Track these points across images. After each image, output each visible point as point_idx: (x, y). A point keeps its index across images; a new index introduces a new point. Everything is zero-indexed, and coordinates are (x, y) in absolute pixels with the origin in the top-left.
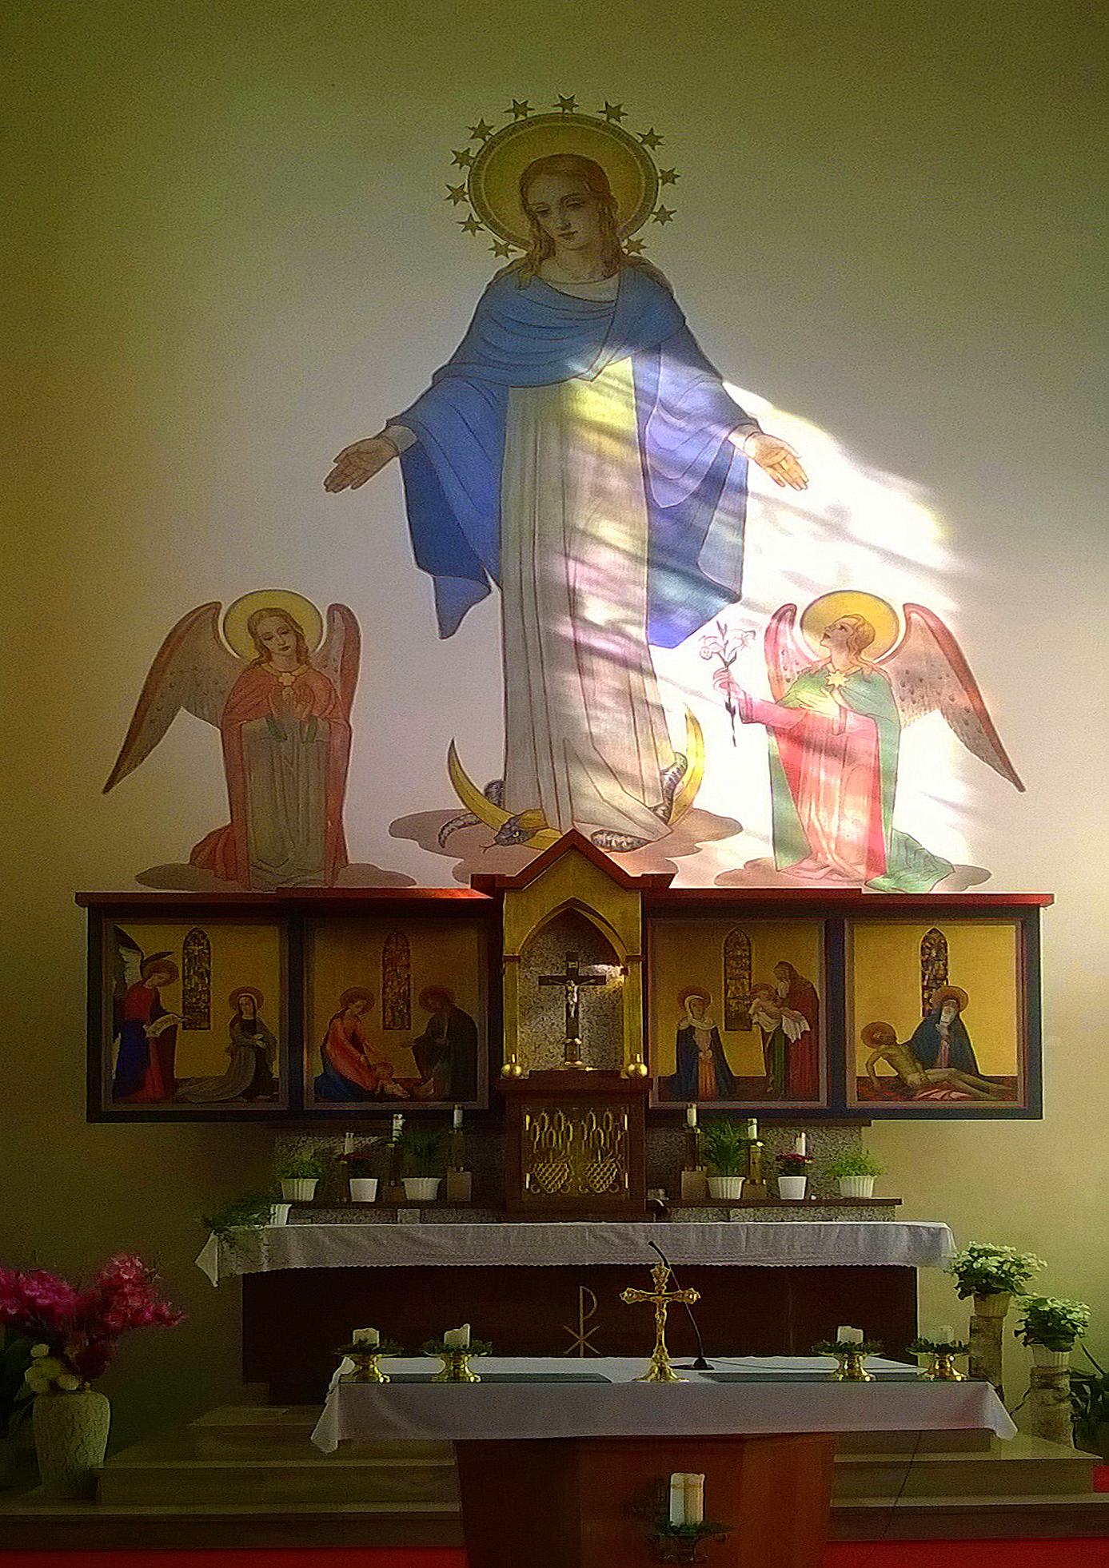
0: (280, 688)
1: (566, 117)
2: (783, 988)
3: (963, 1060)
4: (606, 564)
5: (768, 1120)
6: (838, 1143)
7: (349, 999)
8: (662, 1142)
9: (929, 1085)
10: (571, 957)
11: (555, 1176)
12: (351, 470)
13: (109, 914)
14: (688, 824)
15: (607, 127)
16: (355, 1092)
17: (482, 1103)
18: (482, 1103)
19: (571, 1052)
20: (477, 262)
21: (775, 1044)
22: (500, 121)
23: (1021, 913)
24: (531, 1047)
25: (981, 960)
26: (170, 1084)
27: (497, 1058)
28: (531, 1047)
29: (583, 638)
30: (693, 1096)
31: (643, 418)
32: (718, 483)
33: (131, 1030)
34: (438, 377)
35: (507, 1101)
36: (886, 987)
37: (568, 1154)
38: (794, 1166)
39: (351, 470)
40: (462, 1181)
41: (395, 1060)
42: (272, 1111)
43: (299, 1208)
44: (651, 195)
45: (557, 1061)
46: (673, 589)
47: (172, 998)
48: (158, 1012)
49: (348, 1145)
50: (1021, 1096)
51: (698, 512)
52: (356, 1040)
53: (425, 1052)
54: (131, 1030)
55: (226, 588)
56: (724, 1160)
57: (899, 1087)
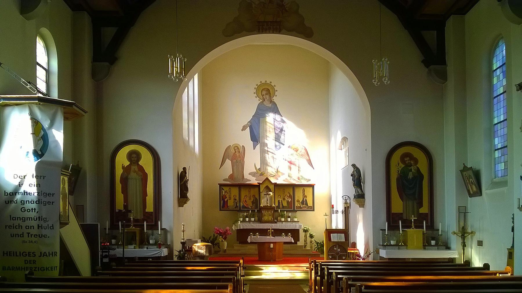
0: (236, 156)
3: (307, 204)
4: (270, 141)
5: (287, 211)
6: (294, 214)
8: (276, 213)
11: (266, 218)
12: (244, 129)
13: (221, 185)
14: (280, 174)
15: (270, 85)
16: (246, 208)
19: (267, 203)
20: (257, 102)
21: (288, 202)
22: (259, 84)
23: (312, 186)
24: (264, 203)
25: (309, 190)
26: (228, 206)
27: (260, 204)
28: (264, 203)
29: (269, 150)
31: (274, 122)
32: (282, 130)
33: (223, 200)
35: (260, 210)
36: (299, 195)
37: (267, 216)
38: (289, 217)
39: (244, 129)
40: (257, 218)
41: (250, 204)
42: (238, 209)
45: (266, 205)
46: (277, 144)
47: (227, 196)
50: (312, 209)
51: (280, 134)
53: (253, 203)
54: (223, 200)
55: (232, 143)
56: (282, 216)
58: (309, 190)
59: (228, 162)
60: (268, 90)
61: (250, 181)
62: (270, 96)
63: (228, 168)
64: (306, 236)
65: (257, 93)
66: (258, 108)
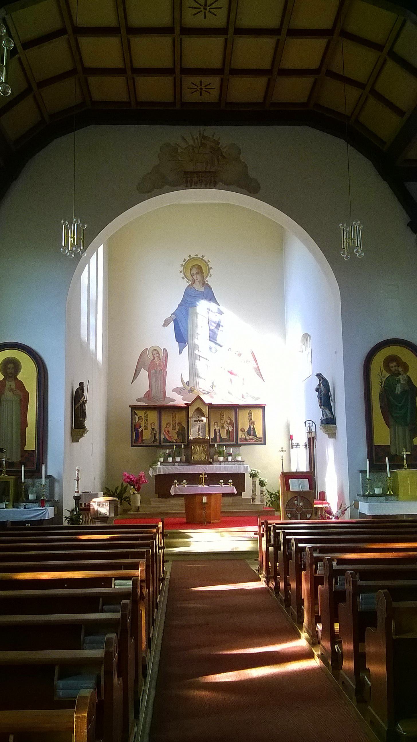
1: (196, 258)
2: (229, 421)
3: (255, 435)
5: (227, 446)
7: (167, 424)
8: (212, 450)
9: (251, 439)
10: (198, 417)
12: (166, 323)
15: (202, 260)
16: (169, 442)
17: (186, 443)
18: (186, 443)
19: (199, 434)
20: (184, 284)
21: (228, 431)
24: (194, 434)
26: (142, 440)
27: (188, 436)
28: (194, 434)
30: (216, 442)
33: (136, 430)
34: (179, 305)
35: (189, 444)
36: (243, 422)
38: (230, 455)
39: (166, 323)
40: (184, 458)
42: (157, 445)
43: (161, 462)
44: (209, 272)
45: (197, 436)
47: (142, 425)
48: (140, 427)
49: (168, 451)
50: (262, 441)
52: (168, 432)
53: (178, 434)
55: (149, 345)
56: (220, 454)
57: (245, 439)
58: (257, 414)
59: (144, 374)
60: (200, 267)
61: (174, 400)
62: (202, 276)
63: (143, 383)
64: (254, 483)
65: (184, 272)
66: (186, 294)
